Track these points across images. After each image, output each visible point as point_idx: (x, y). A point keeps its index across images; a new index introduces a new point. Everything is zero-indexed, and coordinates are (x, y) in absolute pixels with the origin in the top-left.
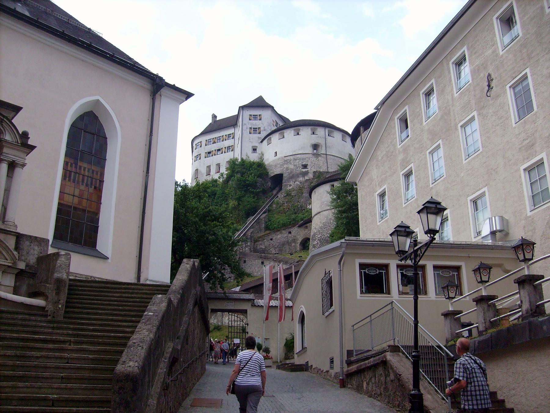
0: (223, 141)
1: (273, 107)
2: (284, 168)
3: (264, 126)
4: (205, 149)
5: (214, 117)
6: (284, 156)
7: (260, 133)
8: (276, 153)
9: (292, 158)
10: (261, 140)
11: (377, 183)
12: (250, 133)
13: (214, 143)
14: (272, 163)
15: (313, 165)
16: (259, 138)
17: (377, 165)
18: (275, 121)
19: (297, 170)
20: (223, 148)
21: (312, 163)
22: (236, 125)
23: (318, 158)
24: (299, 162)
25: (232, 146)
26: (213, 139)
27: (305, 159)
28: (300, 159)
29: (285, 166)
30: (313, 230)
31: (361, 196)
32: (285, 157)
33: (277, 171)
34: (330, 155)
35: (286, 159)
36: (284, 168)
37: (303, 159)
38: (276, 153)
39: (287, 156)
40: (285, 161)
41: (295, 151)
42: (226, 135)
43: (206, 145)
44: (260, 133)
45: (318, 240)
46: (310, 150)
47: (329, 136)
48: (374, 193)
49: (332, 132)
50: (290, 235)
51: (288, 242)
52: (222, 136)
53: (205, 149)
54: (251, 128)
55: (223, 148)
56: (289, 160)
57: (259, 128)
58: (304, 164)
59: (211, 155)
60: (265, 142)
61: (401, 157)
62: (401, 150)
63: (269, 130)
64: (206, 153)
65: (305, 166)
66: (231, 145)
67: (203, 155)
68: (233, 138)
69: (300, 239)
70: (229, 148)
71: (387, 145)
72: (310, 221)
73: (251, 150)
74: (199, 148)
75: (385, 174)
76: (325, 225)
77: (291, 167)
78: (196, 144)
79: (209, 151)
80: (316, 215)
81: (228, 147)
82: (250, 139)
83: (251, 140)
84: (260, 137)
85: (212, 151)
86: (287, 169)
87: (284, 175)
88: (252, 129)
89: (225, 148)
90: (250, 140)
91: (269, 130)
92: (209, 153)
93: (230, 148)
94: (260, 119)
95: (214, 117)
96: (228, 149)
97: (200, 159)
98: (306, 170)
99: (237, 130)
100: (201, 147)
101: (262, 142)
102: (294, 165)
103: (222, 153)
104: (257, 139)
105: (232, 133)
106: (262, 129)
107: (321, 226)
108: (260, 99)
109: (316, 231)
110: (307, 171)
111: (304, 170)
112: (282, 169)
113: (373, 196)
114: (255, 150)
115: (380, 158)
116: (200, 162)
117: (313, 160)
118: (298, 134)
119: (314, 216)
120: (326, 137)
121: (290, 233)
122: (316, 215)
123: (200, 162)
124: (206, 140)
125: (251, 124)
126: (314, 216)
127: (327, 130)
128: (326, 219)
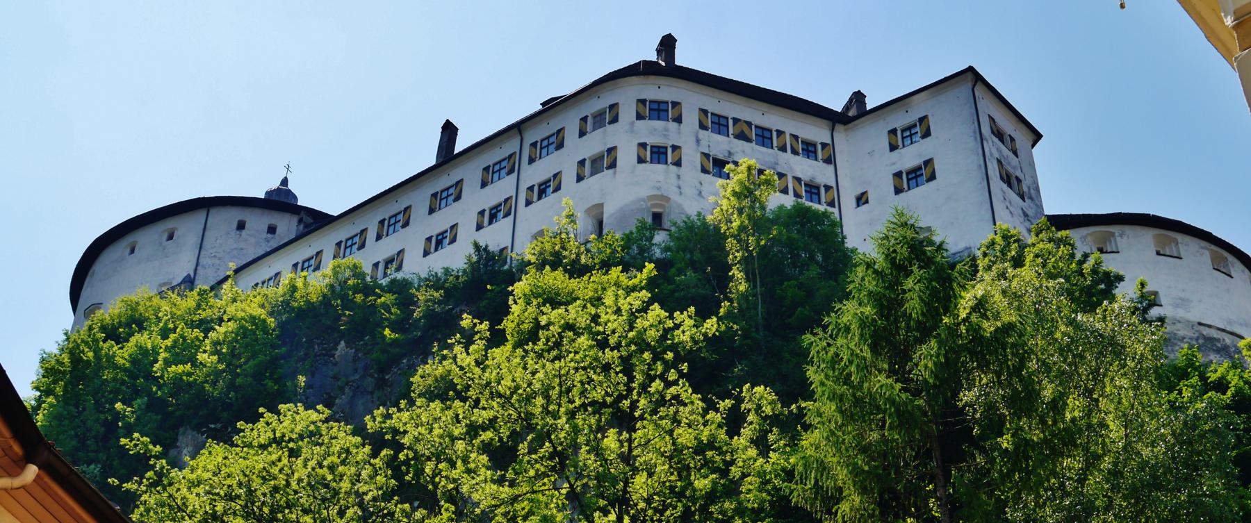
4: (698, 141)
5: (667, 44)
6: (1198, 320)
13: (742, 136)
32: (1200, 324)
35: (1206, 331)
39: (1210, 326)
41: (1230, 322)
53: (698, 141)
56: (1218, 340)
79: (721, 157)
89: (798, 180)
93: (813, 190)
95: (667, 44)
116: (679, 177)
123: (679, 177)
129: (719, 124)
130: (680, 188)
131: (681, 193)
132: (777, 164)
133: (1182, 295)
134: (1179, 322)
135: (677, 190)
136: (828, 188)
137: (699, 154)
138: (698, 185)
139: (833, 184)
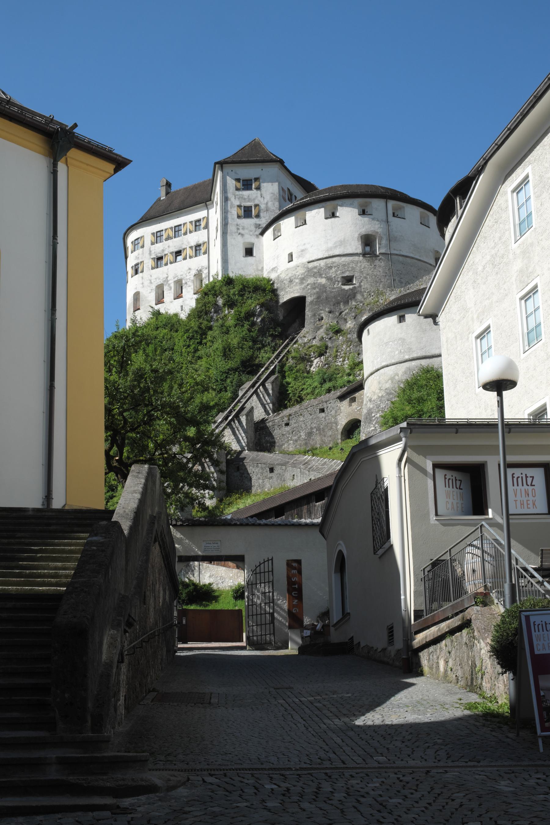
0: (185, 234)
1: (281, 162)
2: (308, 285)
3: (266, 201)
4: (150, 251)
7: (258, 216)
8: (291, 256)
9: (322, 263)
10: (260, 230)
11: (475, 316)
13: (169, 238)
14: (283, 276)
15: (366, 278)
16: (258, 226)
17: (475, 282)
18: (286, 190)
19: (334, 288)
20: (186, 248)
21: (361, 272)
22: (210, 200)
23: (373, 262)
24: (336, 271)
25: (204, 243)
26: (166, 230)
27: (348, 264)
28: (338, 266)
29: (311, 280)
30: (366, 405)
31: (447, 341)
32: (309, 262)
34: (397, 255)
35: (311, 265)
36: (308, 285)
37: (344, 265)
38: (291, 256)
40: (309, 270)
42: (191, 222)
43: (152, 244)
44: (258, 216)
45: (376, 423)
46: (356, 247)
47: (394, 215)
48: (470, 333)
49: (400, 208)
51: (318, 429)
52: (184, 224)
53: (150, 251)
54: (239, 206)
55: (186, 248)
56: (315, 267)
57: (256, 206)
58: (347, 274)
59: (164, 261)
60: (269, 233)
61: (518, 265)
62: (518, 251)
63: (275, 209)
64: (153, 259)
65: (348, 280)
66: (201, 242)
67: (149, 263)
68: (207, 227)
69: (342, 421)
70: (198, 248)
71: (493, 244)
72: (360, 387)
73: (242, 252)
74: (139, 251)
75: (488, 299)
77: (323, 281)
78: (132, 243)
79: (159, 255)
80: (372, 374)
81: (196, 247)
82: (238, 229)
83: (241, 231)
84: (258, 223)
85: (165, 255)
86: (314, 286)
87: (309, 300)
88: (242, 208)
89: (191, 247)
90: (239, 232)
91: (275, 209)
92: (160, 259)
96: (196, 250)
98: (351, 287)
99: (212, 211)
100: (143, 247)
101: (262, 233)
102: (329, 279)
103: (185, 259)
104: (253, 228)
105: (204, 218)
107: (382, 396)
108: (255, 146)
109: (371, 406)
110: (355, 287)
111: (347, 287)
112: (303, 286)
113: (468, 339)
114: (249, 252)
115: (480, 268)
117: (365, 267)
119: (367, 378)
120: (389, 220)
122: (372, 374)
123: (142, 278)
124: (153, 234)
125: (239, 199)
126: (367, 378)
127: (391, 203)
128: (390, 382)
129: (158, 237)
130: (143, 284)
131: (143, 286)
132: (183, 244)
133: (303, 248)
134: (298, 266)
135: (141, 285)
137: (151, 260)
138: (150, 278)
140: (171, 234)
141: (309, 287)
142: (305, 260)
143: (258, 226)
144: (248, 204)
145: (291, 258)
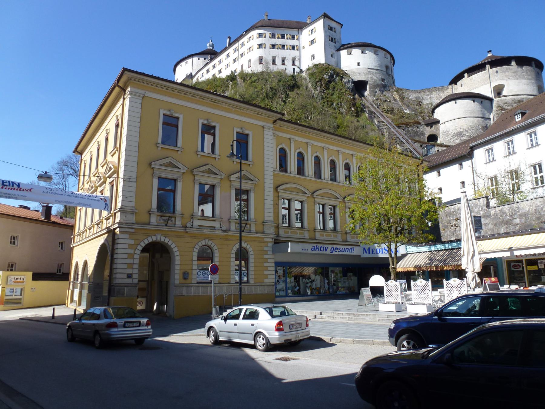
8: (358, 64)
9: (374, 71)
12: (330, 40)
13: (278, 38)
14: (354, 71)
32: (368, 68)
33: (363, 78)
40: (369, 72)
44: (335, 43)
50: (418, 130)
57: (335, 39)
66: (295, 44)
67: (268, 46)
69: (427, 135)
76: (472, 127)
77: (375, 78)
86: (372, 78)
89: (290, 45)
94: (335, 32)
97: (265, 48)
100: (265, 37)
106: (336, 40)
112: (366, 77)
118: (351, 54)
121: (418, 127)
128: (472, 123)
129: (273, 36)
136: (297, 46)
139: (298, 45)
140: (280, 37)
141: (369, 78)
142: (367, 67)
143: (335, 47)
144: (332, 37)
145: (358, 64)
